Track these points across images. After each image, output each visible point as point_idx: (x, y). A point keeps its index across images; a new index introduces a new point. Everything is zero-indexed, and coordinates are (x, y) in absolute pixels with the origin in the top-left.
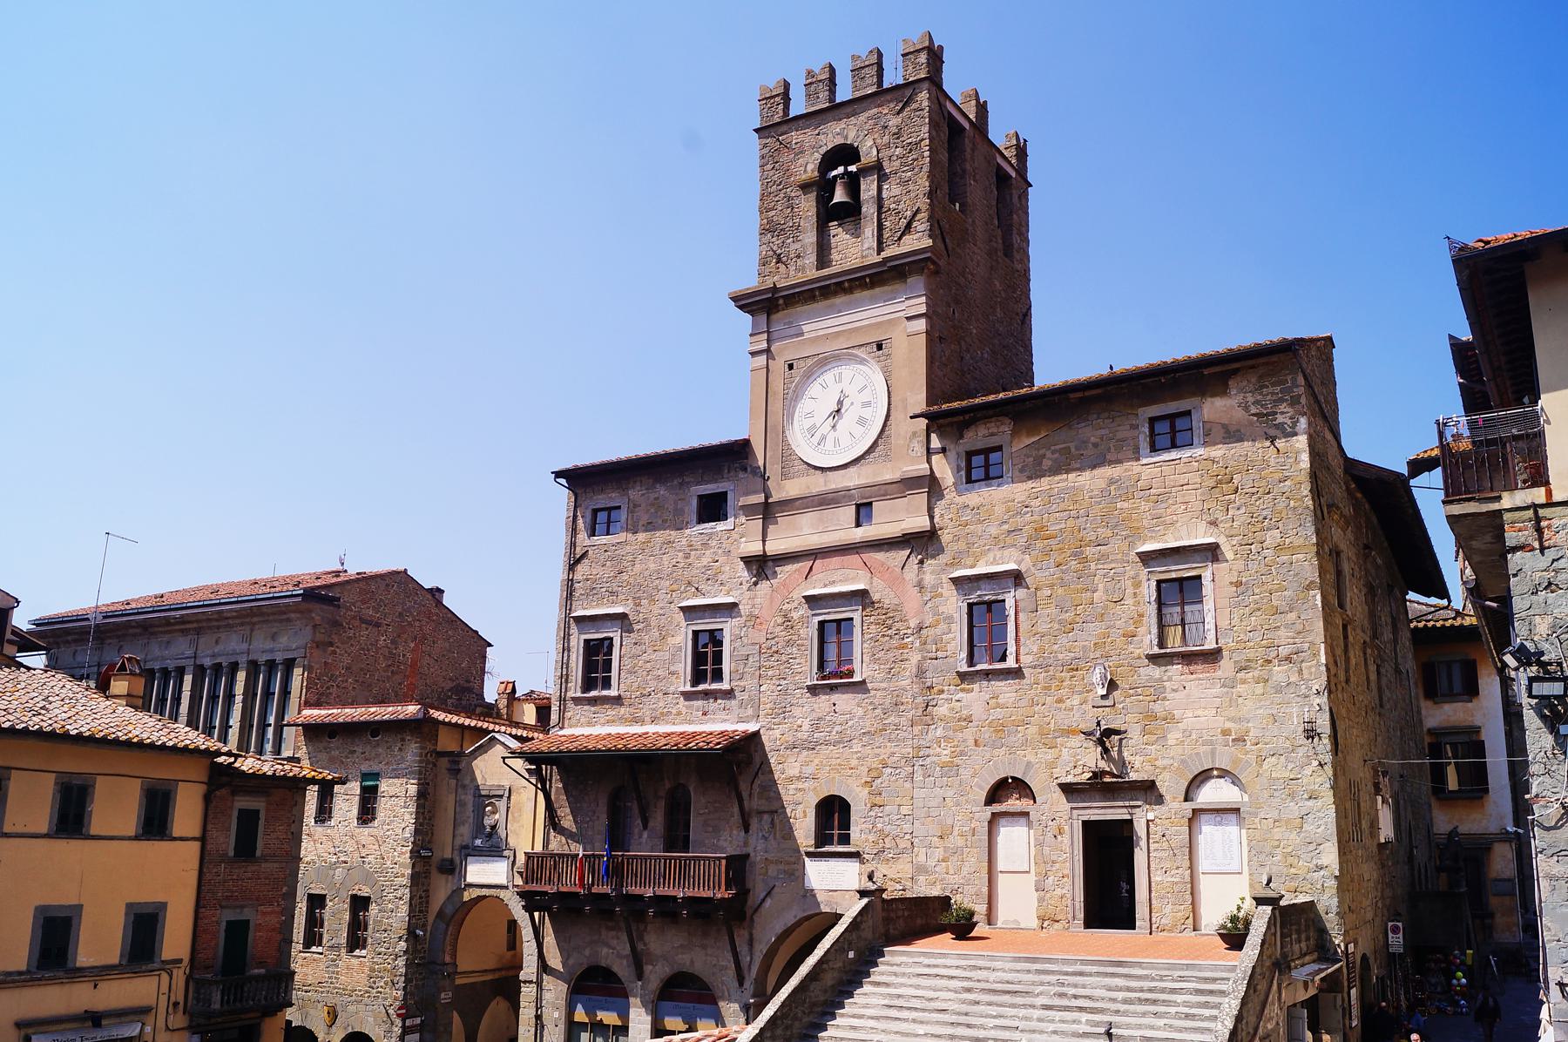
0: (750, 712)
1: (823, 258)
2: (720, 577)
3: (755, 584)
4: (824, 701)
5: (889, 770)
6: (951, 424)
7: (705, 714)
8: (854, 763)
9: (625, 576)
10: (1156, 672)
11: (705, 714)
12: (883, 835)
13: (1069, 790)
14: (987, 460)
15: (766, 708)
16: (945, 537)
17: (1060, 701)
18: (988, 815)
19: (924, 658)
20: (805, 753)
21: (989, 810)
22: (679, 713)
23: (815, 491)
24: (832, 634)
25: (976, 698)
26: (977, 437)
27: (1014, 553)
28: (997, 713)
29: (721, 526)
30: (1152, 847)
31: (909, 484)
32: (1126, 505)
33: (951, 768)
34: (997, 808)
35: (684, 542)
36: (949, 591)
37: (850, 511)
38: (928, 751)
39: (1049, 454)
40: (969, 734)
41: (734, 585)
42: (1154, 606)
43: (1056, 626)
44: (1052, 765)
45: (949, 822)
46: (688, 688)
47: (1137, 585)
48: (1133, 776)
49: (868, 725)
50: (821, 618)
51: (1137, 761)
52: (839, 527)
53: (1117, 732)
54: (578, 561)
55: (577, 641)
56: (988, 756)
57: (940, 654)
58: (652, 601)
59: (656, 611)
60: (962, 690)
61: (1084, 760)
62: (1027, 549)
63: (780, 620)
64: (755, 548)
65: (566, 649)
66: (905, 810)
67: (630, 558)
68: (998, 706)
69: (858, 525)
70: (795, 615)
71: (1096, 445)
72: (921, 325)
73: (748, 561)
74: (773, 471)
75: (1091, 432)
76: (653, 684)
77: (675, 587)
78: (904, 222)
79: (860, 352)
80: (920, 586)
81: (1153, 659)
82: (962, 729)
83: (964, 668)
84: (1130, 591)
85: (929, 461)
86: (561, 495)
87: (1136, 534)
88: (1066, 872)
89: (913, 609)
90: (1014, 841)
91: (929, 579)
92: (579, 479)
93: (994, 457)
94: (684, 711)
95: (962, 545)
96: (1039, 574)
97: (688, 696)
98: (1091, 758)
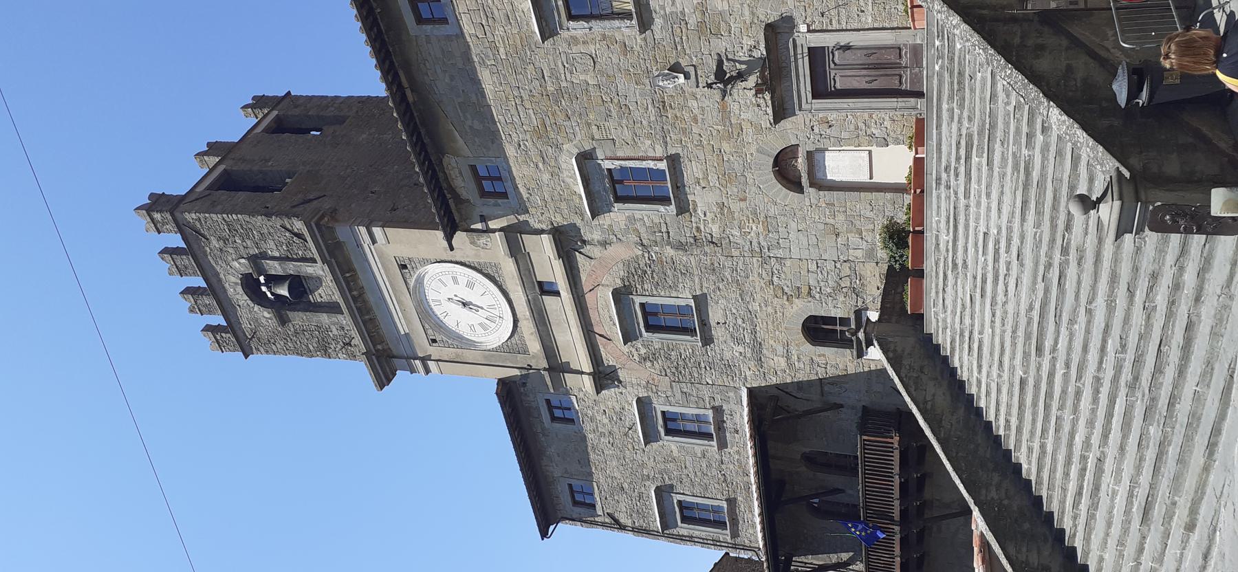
0: (731, 394)
1: (332, 308)
2: (617, 409)
3: (620, 382)
4: (718, 333)
5: (775, 279)
6: (459, 210)
7: (737, 432)
8: (770, 310)
9: (626, 486)
11: (737, 432)
12: (838, 288)
13: (781, 112)
14: (485, 178)
15: (727, 381)
16: (559, 220)
17: (695, 120)
18: (812, 190)
19: (669, 243)
20: (765, 351)
22: (738, 452)
23: (534, 330)
24: (656, 320)
25: (702, 199)
26: (464, 186)
27: (563, 158)
28: (713, 178)
30: (835, 26)
31: (515, 250)
32: (502, 50)
33: (769, 224)
34: (805, 181)
36: (605, 220)
37: (548, 300)
38: (755, 243)
39: (469, 123)
40: (735, 206)
41: (621, 402)
42: (593, 23)
43: (624, 121)
44: (759, 129)
45: (821, 227)
46: (714, 443)
47: (575, 39)
48: (761, 51)
49: (734, 295)
50: (643, 330)
51: (748, 42)
52: (561, 308)
53: (720, 63)
54: (617, 521)
55: (684, 529)
56: (754, 189)
57: (664, 230)
58: (643, 465)
59: (651, 463)
60: (695, 211)
61: (747, 102)
62: (558, 147)
63: (649, 364)
64: (588, 382)
65: (690, 539)
66: (813, 267)
67: (609, 480)
68: (706, 178)
69: (557, 294)
70: (643, 351)
71: (452, 78)
72: (377, 231)
73: (599, 388)
74: (522, 360)
75: (440, 83)
76: (714, 472)
77: (630, 447)
79: (412, 283)
80: (604, 244)
81: (645, 24)
82: (732, 213)
83: (672, 208)
84: (582, 48)
85: (494, 231)
86: (564, 531)
87: (526, 38)
88: (866, 116)
89: (621, 252)
90: (842, 165)
91: (596, 236)
92: (546, 519)
93: (483, 172)
94: (735, 448)
95: (563, 205)
96: (579, 137)
97: (722, 445)
98: (744, 92)
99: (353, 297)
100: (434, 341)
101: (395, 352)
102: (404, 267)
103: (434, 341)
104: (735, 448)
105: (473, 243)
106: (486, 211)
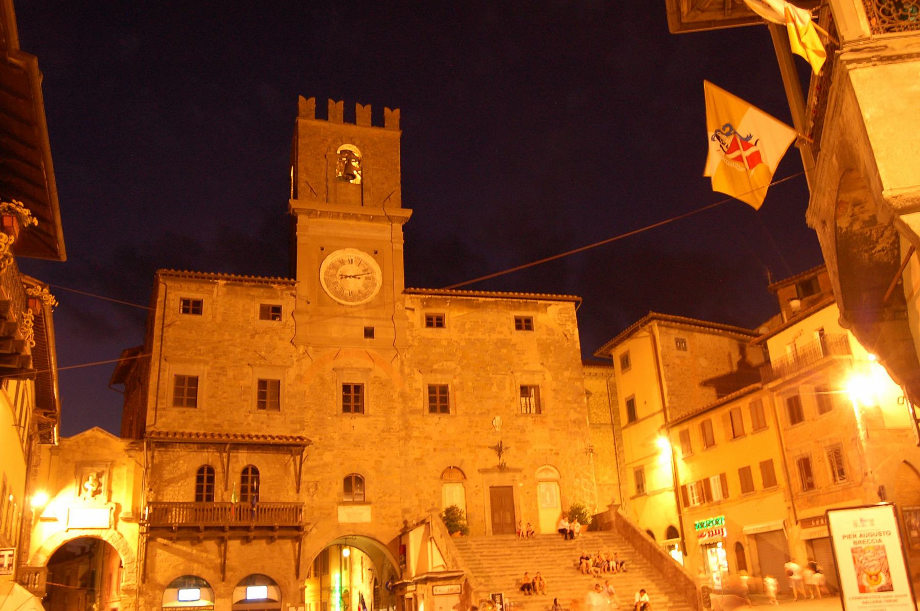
0: (298, 427)
10: (521, 421)
17: (477, 433)
20: (335, 452)
21: (442, 482)
32: (504, 351)
33: (419, 461)
35: (250, 328)
70: (328, 378)
80: (402, 371)
91: (407, 370)
94: (253, 423)
95: (426, 357)
103: (322, 249)
104: (253, 423)
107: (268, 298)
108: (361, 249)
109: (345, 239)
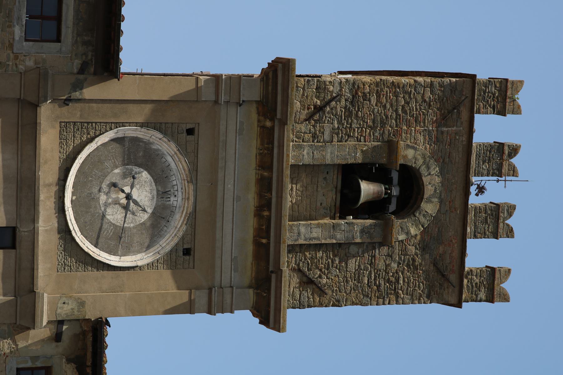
29: (18, 32)
74: (73, 113)
78: (315, 274)
99: (270, 210)
100: (190, 132)
101: (253, 109)
102: (187, 252)
103: (190, 132)
105: (82, 304)
106: (52, 349)
107: (77, 11)
108: (192, 219)
109: (214, 184)
